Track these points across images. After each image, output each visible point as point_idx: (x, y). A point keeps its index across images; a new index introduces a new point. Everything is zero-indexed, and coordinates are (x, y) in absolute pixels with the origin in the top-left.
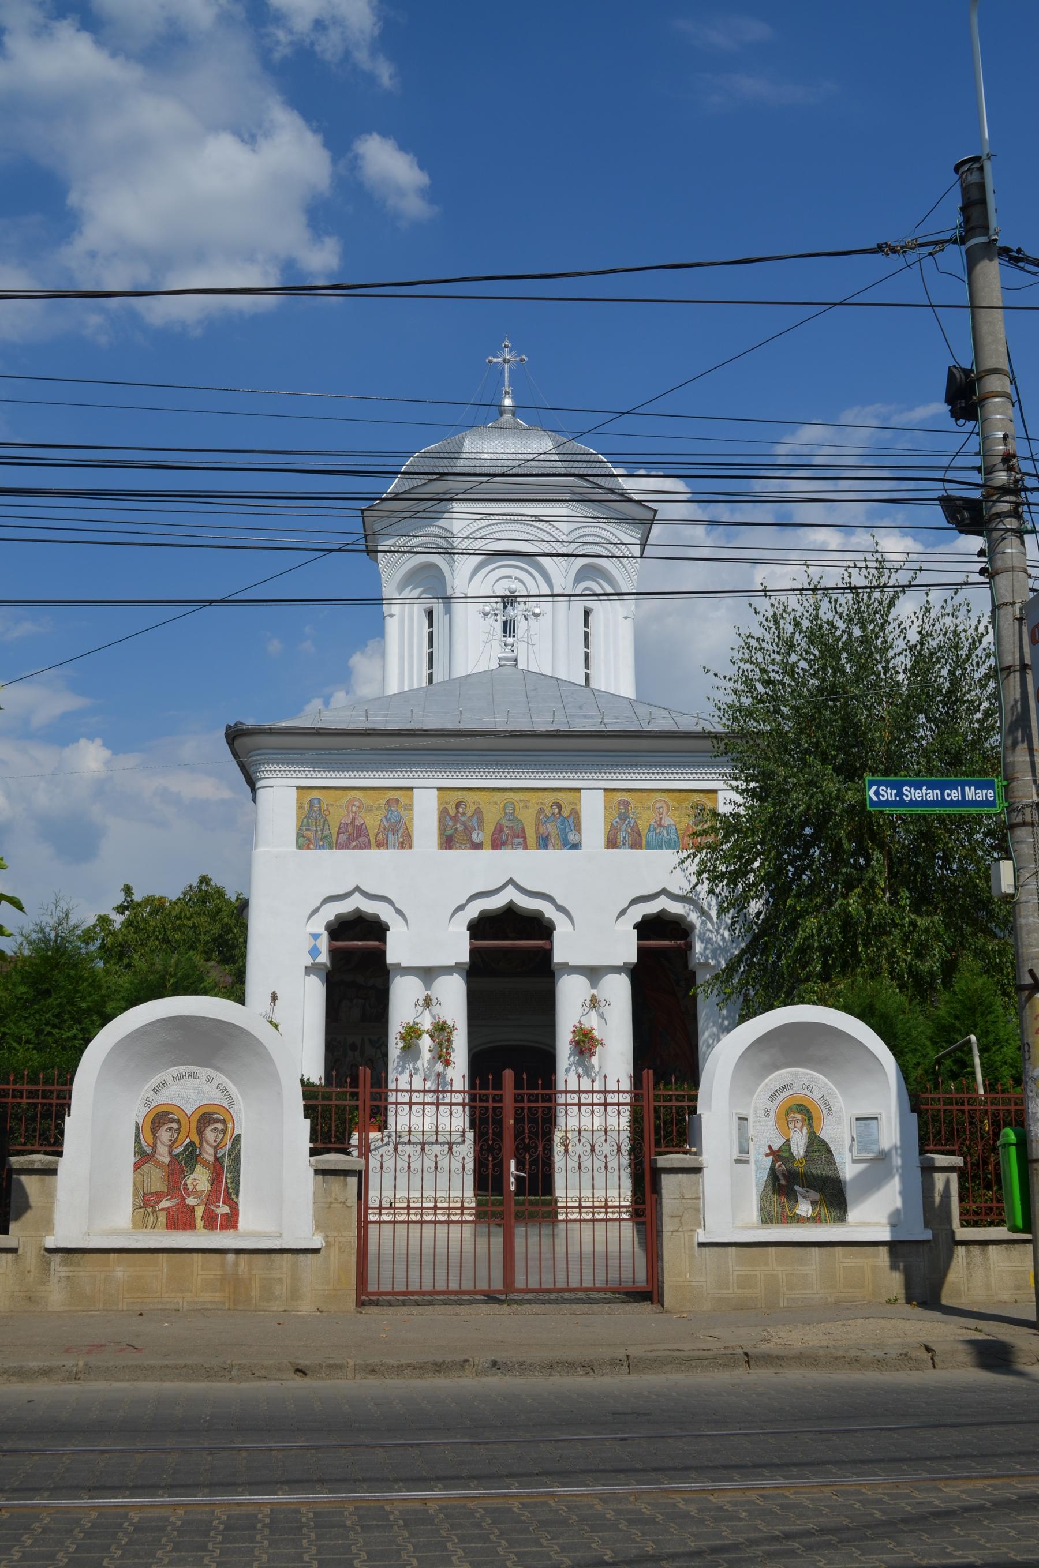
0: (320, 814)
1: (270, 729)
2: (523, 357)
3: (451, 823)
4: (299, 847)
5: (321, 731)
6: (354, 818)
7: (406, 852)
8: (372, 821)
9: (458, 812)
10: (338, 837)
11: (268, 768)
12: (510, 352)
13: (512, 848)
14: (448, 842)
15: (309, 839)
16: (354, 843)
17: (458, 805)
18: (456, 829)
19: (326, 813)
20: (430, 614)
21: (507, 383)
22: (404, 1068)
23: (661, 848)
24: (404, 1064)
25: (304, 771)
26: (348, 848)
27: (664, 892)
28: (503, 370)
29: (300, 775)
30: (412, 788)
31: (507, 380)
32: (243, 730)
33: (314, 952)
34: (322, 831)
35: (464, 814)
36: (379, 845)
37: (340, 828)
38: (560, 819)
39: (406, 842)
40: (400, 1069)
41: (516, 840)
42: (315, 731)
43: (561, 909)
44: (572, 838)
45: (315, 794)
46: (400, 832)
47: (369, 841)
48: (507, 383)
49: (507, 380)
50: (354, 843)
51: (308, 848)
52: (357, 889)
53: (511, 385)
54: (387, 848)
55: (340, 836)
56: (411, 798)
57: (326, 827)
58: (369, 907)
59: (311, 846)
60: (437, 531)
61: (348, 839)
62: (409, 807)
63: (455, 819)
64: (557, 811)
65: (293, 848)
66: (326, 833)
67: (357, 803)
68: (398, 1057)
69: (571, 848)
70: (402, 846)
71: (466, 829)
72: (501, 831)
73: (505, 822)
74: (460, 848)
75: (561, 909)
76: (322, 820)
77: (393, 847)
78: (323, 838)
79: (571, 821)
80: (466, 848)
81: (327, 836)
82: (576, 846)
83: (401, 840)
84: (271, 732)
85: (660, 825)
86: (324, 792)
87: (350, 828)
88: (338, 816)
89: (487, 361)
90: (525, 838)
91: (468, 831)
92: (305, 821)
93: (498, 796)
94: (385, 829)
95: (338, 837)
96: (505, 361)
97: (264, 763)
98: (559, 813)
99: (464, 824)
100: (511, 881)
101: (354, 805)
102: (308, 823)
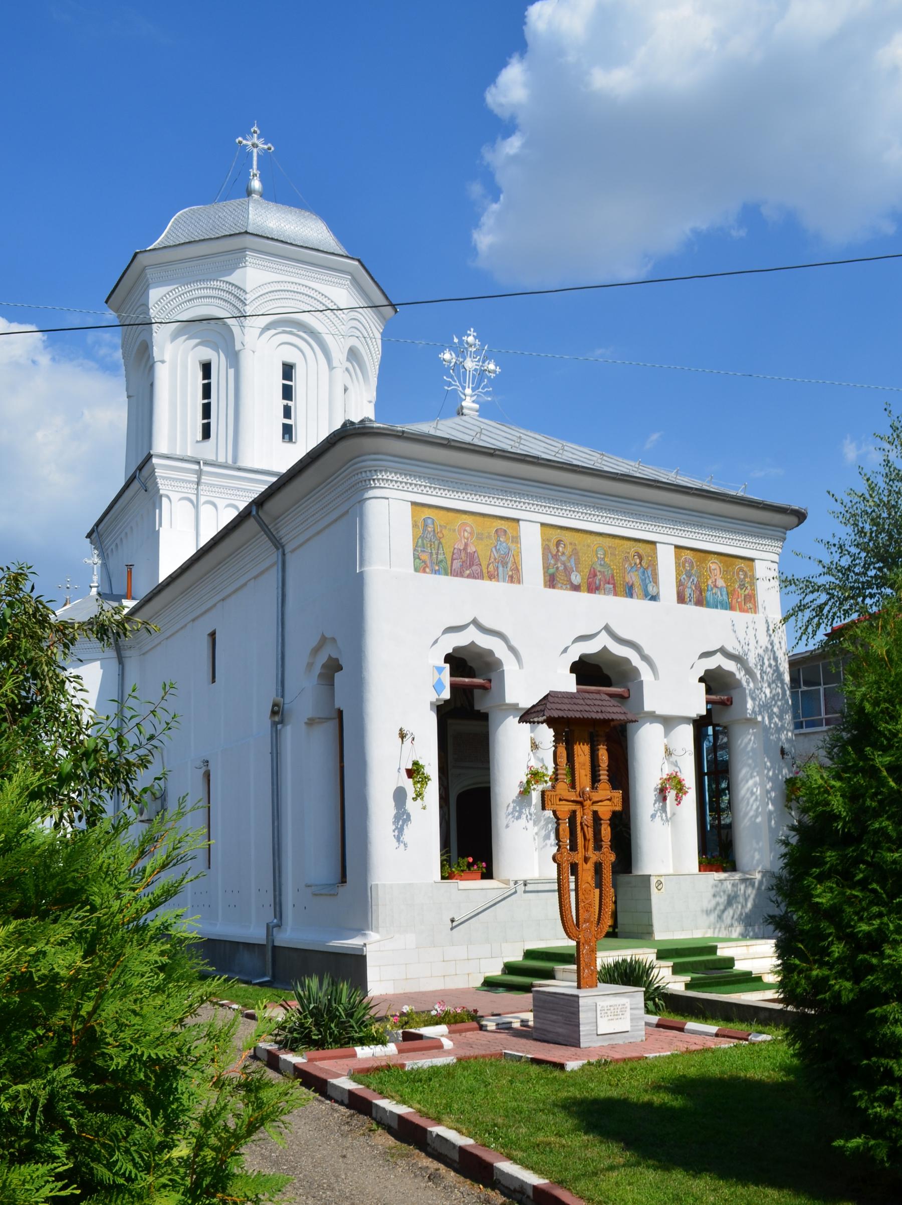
0: (434, 535)
1: (403, 432)
2: (270, 145)
3: (552, 562)
4: (416, 570)
5: (453, 444)
6: (466, 545)
7: (514, 587)
8: (481, 549)
9: (558, 551)
10: (452, 563)
11: (385, 477)
12: (258, 138)
13: (605, 594)
14: (551, 581)
15: (424, 562)
16: (468, 572)
18: (557, 568)
19: (441, 535)
20: (206, 369)
21: (255, 166)
22: (521, 813)
23: (717, 607)
24: (521, 809)
25: (420, 486)
27: (723, 651)
29: (415, 490)
30: (518, 520)
32: (373, 428)
33: (438, 687)
34: (437, 554)
35: (563, 554)
36: (491, 577)
37: (453, 554)
38: (641, 570)
39: (515, 577)
40: (517, 814)
41: (607, 586)
42: (445, 442)
43: (645, 658)
44: (651, 589)
45: (427, 513)
46: (510, 565)
47: (481, 570)
48: (255, 166)
50: (468, 572)
51: (424, 571)
52: (475, 622)
53: (258, 169)
54: (498, 581)
55: (455, 562)
56: (517, 530)
57: (441, 551)
58: (485, 642)
59: (427, 570)
60: (224, 286)
61: (462, 566)
62: (516, 539)
63: (555, 557)
64: (638, 561)
66: (441, 557)
67: (468, 529)
68: (514, 801)
69: (650, 599)
70: (511, 580)
71: (565, 568)
72: (595, 575)
73: (599, 568)
74: (561, 588)
75: (645, 658)
76: (436, 542)
77: (504, 581)
78: (439, 563)
80: (566, 589)
81: (441, 561)
82: (654, 598)
83: (510, 573)
84: (402, 436)
85: (716, 586)
86: (436, 511)
87: (463, 555)
88: (452, 542)
89: (237, 141)
90: (614, 584)
91: (568, 571)
92: (420, 541)
93: (590, 539)
94: (495, 559)
95: (452, 563)
96: (255, 145)
97: (381, 471)
98: (640, 563)
99: (564, 564)
100: (607, 629)
101: (465, 530)
102: (423, 544)
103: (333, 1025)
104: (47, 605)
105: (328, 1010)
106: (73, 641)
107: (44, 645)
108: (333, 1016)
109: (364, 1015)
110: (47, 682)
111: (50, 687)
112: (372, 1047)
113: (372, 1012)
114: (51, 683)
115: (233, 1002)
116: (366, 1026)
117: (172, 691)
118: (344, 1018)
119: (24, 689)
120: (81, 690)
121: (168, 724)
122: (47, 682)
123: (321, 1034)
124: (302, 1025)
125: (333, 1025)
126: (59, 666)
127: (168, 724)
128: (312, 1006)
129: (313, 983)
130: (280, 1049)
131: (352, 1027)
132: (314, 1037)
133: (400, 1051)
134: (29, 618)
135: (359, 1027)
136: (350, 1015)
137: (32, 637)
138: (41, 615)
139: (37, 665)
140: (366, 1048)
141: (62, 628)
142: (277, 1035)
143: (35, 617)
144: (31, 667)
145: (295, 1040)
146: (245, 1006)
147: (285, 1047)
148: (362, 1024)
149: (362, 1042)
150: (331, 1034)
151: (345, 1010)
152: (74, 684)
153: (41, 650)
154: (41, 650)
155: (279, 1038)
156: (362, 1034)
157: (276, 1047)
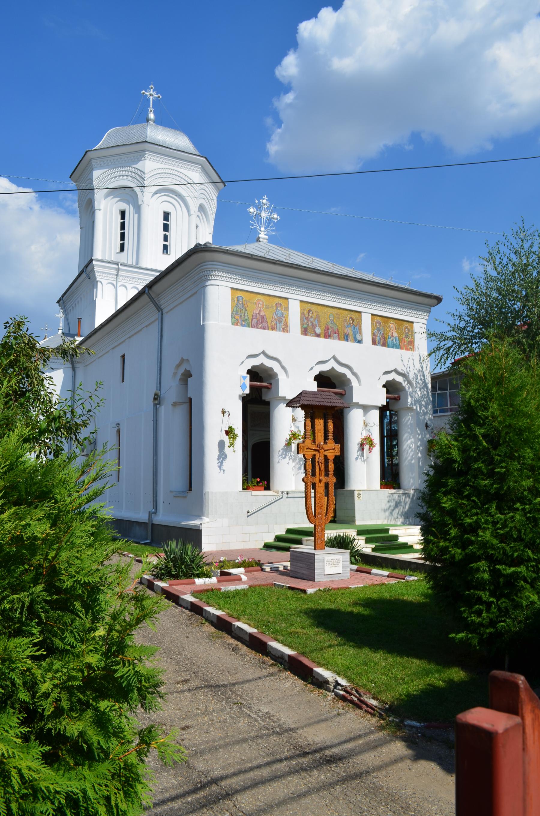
0: (243, 306)
1: (227, 250)
3: (306, 321)
4: (233, 324)
5: (254, 257)
6: (260, 311)
7: (285, 334)
8: (268, 314)
12: (153, 91)
14: (305, 332)
16: (260, 326)
17: (309, 311)
18: (308, 325)
19: (246, 306)
20: (123, 214)
21: (151, 106)
22: (286, 455)
23: (393, 347)
24: (286, 453)
26: (257, 328)
27: (396, 371)
28: (149, 100)
29: (233, 281)
30: (288, 299)
31: (151, 104)
32: (211, 247)
33: (243, 387)
34: (244, 316)
35: (312, 317)
36: (273, 329)
38: (353, 327)
39: (285, 329)
41: (335, 335)
42: (250, 256)
43: (354, 374)
44: (358, 337)
45: (239, 294)
46: (283, 322)
47: (268, 325)
48: (151, 106)
49: (151, 104)
50: (260, 326)
51: (237, 325)
52: (264, 353)
53: (153, 107)
54: (276, 331)
59: (239, 324)
60: (133, 170)
61: (257, 322)
62: (287, 309)
63: (307, 319)
64: (351, 322)
65: (230, 324)
66: (246, 317)
67: (261, 303)
68: (282, 449)
69: (358, 342)
70: (284, 330)
71: (313, 325)
72: (328, 329)
73: (330, 325)
74: (310, 335)
75: (354, 374)
77: (280, 331)
78: (245, 320)
79: (357, 328)
80: (313, 336)
81: (246, 320)
82: (360, 342)
85: (392, 336)
86: (244, 293)
87: (258, 316)
88: (252, 310)
91: (314, 326)
93: (326, 309)
96: (151, 95)
97: (215, 271)
99: (312, 322)
100: (334, 357)
103: (183, 567)
104: (35, 338)
105: (181, 559)
106: (48, 358)
107: (33, 360)
108: (183, 562)
109: (200, 562)
110: (34, 380)
111: (36, 382)
112: (204, 579)
113: (204, 560)
114: (36, 380)
115: (130, 553)
116: (200, 568)
117: (101, 386)
118: (189, 563)
119: (22, 384)
120: (52, 384)
121: (98, 404)
122: (34, 380)
123: (176, 571)
124: (166, 566)
125: (183, 567)
126: (40, 372)
127: (98, 404)
128: (172, 556)
129: (173, 544)
130: (154, 579)
131: (193, 568)
132: (173, 573)
133: (219, 581)
134: (25, 345)
135: (197, 568)
136: (192, 562)
137: (26, 356)
138: (32, 344)
139: (29, 371)
140: (201, 580)
141: (43, 351)
142: (153, 571)
143: (28, 345)
144: (26, 372)
145: (162, 574)
146: (136, 555)
147: (157, 578)
148: (199, 566)
149: (198, 576)
150: (182, 571)
151: (190, 559)
152: (48, 381)
153: (31, 362)
154: (31, 362)
155: (154, 573)
156: (198, 572)
157: (152, 578)
